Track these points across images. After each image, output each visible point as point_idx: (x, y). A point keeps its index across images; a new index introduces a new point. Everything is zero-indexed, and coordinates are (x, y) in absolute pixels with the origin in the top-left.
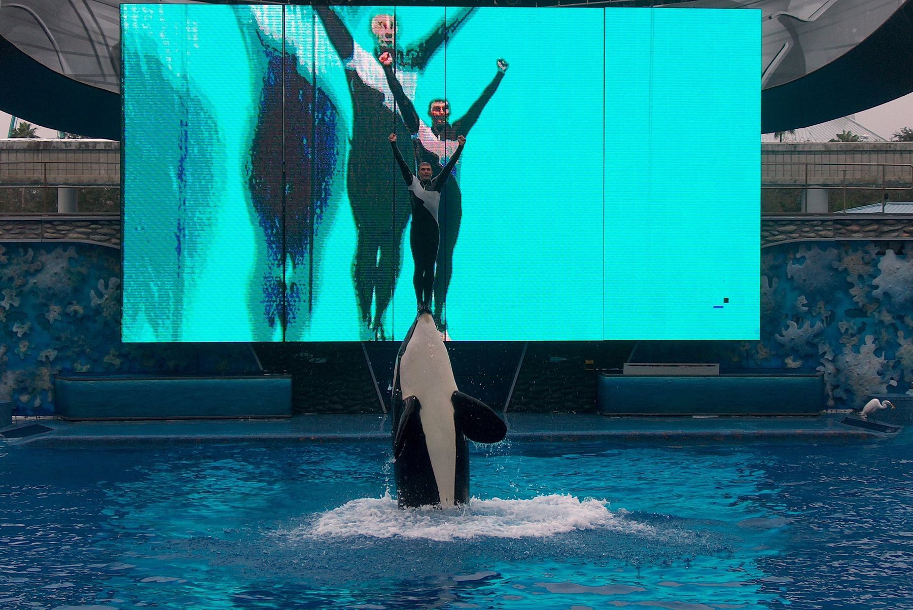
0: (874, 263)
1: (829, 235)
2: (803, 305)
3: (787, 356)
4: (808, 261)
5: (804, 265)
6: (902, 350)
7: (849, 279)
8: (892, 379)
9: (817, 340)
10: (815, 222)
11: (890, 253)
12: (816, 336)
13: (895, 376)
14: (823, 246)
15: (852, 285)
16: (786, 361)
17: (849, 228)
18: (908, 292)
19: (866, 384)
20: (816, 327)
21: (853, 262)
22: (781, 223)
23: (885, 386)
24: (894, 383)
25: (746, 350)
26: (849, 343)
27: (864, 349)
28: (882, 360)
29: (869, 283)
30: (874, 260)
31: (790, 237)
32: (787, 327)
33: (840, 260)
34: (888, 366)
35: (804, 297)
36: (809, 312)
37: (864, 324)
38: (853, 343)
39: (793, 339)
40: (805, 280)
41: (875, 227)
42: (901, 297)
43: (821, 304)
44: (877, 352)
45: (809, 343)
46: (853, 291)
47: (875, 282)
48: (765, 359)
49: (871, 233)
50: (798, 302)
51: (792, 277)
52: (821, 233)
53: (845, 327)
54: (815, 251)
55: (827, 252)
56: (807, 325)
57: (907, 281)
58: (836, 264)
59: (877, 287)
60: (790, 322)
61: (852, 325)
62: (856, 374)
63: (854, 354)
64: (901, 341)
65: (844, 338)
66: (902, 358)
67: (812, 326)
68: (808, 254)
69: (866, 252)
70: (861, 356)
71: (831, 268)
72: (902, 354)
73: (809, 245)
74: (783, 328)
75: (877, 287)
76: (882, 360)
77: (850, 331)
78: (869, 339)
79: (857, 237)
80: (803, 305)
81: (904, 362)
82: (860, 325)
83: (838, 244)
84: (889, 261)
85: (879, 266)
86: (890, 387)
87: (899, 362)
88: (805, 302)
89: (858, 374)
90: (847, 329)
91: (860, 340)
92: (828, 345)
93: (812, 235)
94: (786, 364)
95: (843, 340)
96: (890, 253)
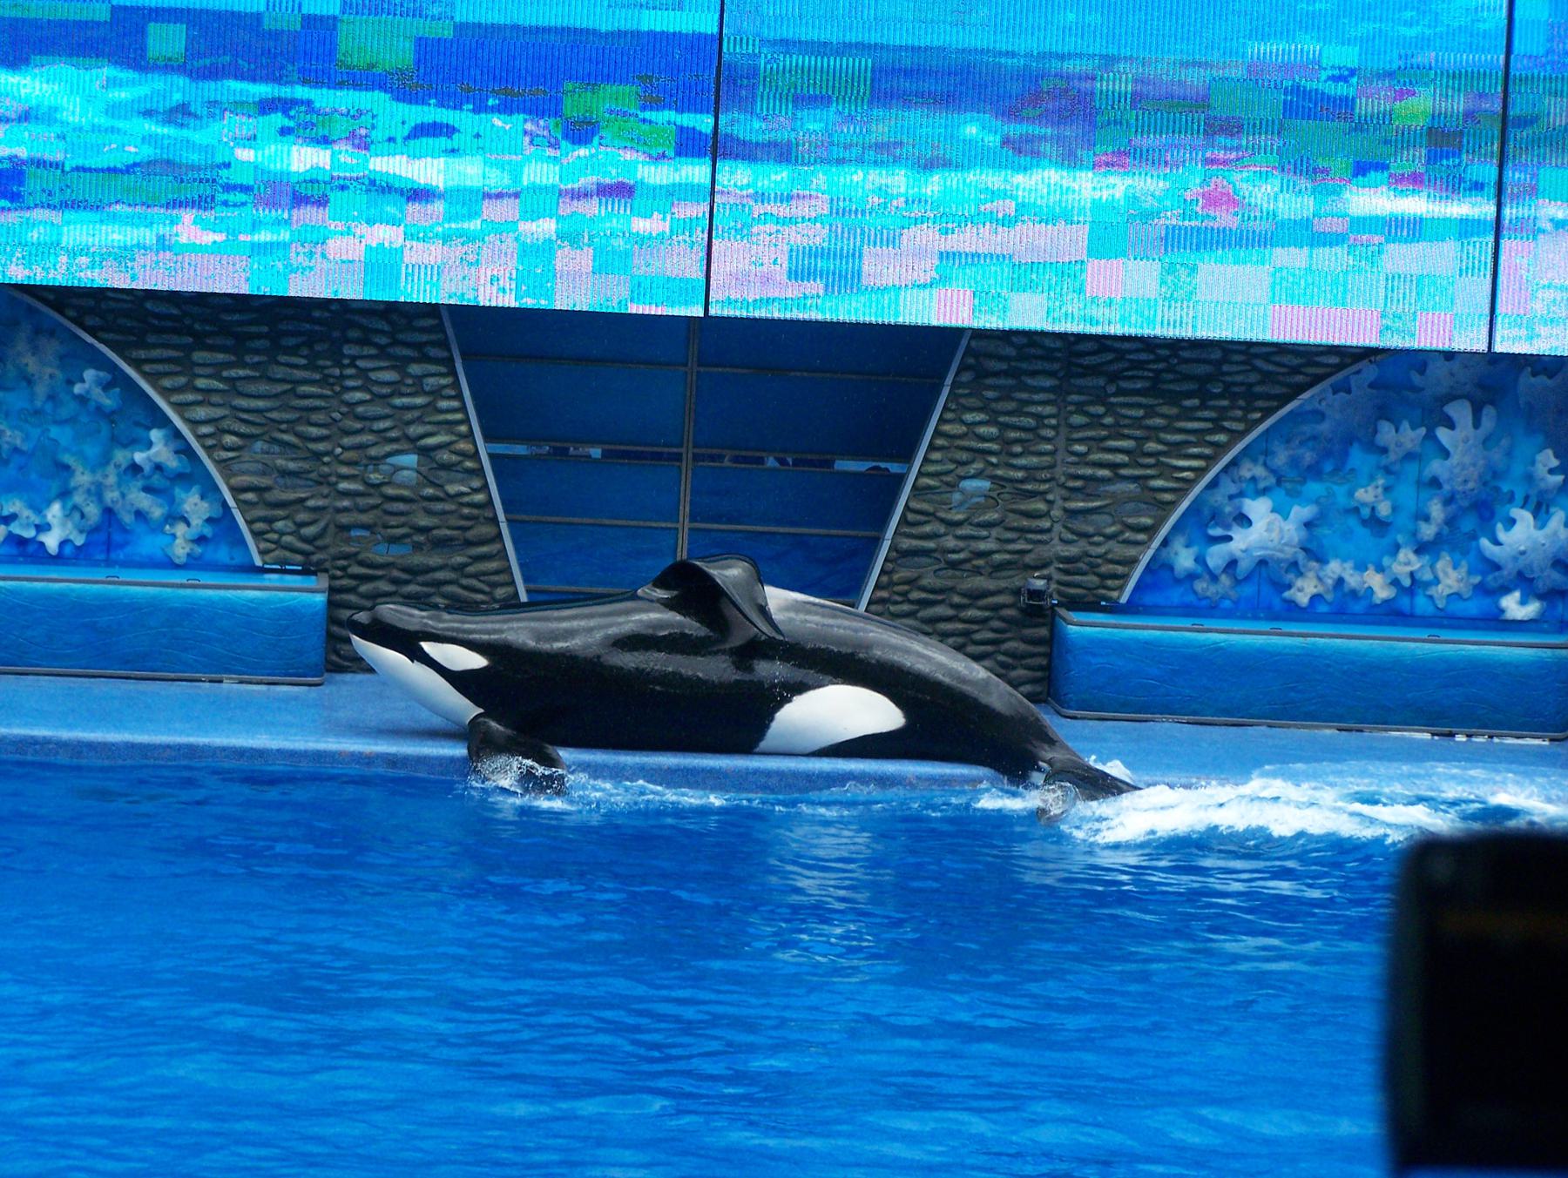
2: (1551, 471)
3: (1506, 590)
5: (1559, 379)
25: (1412, 574)
32: (1513, 522)
35: (1550, 452)
39: (1523, 553)
48: (1456, 596)
60: (1516, 512)
74: (1499, 526)
80: (1551, 471)
88: (1555, 463)
94: (1502, 611)
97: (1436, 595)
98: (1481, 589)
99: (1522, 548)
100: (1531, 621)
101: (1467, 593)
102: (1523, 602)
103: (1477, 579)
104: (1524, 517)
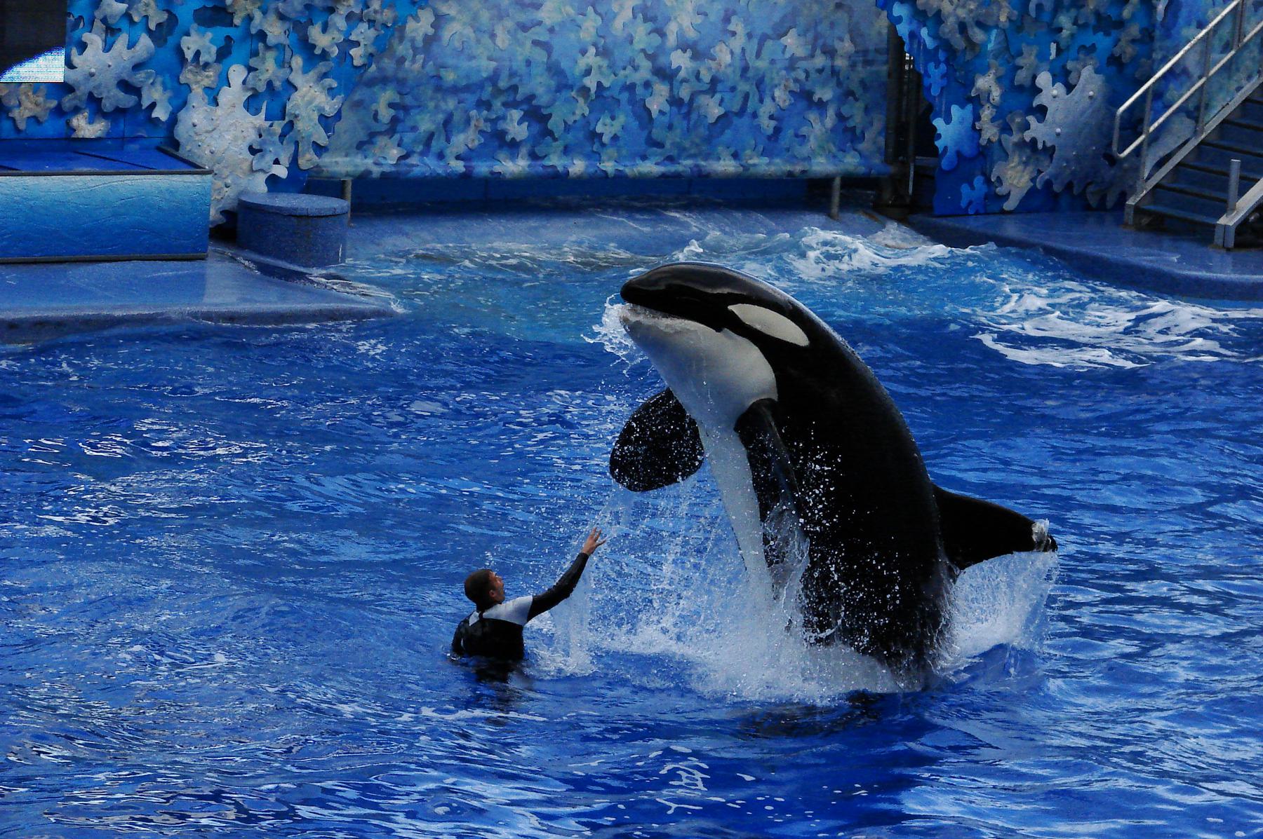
3: (76, 110)
6: (297, 98)
8: (277, 162)
9: (140, 76)
12: (137, 67)
13: (285, 159)
19: (226, 172)
20: (138, 48)
23: (261, 179)
24: (281, 171)
26: (197, 82)
27: (226, 96)
28: (260, 120)
34: (272, 134)
36: (127, 16)
37: (228, 38)
38: (206, 82)
39: (92, 75)
44: (251, 104)
48: (35, 119)
53: (194, 48)
56: (121, 41)
61: (207, 43)
62: (207, 152)
63: (208, 108)
64: (297, 79)
65: (190, 71)
66: (296, 116)
67: (131, 45)
70: (219, 111)
72: (297, 106)
76: (260, 120)
77: (203, 59)
78: (237, 74)
81: (299, 125)
82: (222, 44)
86: (273, 181)
87: (291, 124)
89: (212, 153)
90: (198, 54)
91: (219, 75)
92: (159, 88)
95: (187, 76)
98: (59, 112)
99: (93, 70)
100: (98, 139)
101: (44, 116)
102: (91, 122)
103: (53, 104)
104: (95, 40)
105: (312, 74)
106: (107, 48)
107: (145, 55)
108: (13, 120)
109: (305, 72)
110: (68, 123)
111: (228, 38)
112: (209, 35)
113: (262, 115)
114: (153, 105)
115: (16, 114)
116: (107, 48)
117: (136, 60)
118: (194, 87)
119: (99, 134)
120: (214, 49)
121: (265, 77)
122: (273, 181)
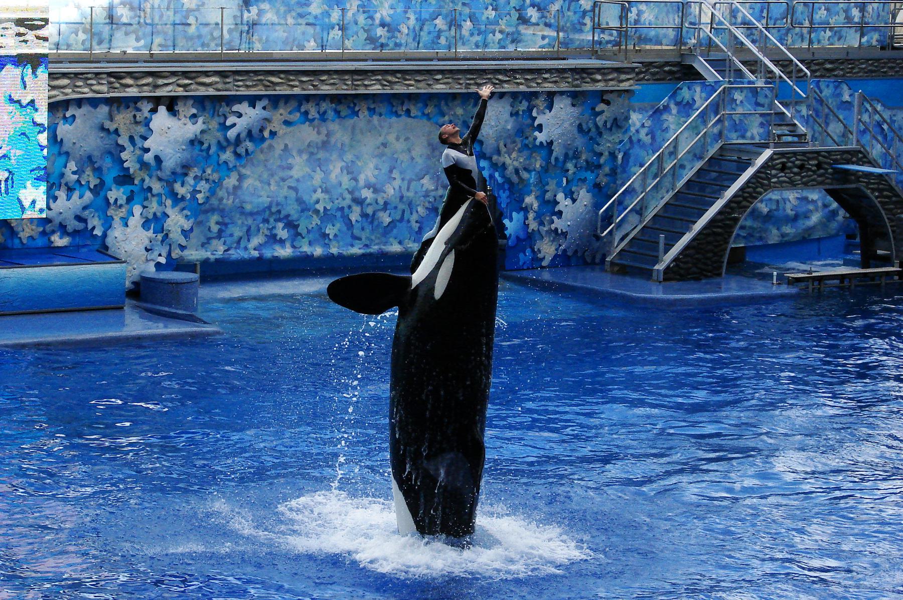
0: (147, 123)
1: (103, 89)
2: (74, 173)
3: (53, 232)
4: (78, 120)
7: (120, 142)
8: (160, 255)
9: (87, 212)
10: (89, 76)
11: (162, 109)
12: (85, 208)
13: (164, 254)
14: (94, 103)
15: (123, 149)
16: (53, 238)
17: (124, 81)
18: (179, 155)
19: (133, 262)
20: (85, 198)
21: (123, 119)
22: (54, 76)
23: (152, 264)
24: (163, 260)
26: (116, 215)
27: (132, 221)
28: (150, 233)
29: (140, 146)
30: (146, 118)
31: (63, 93)
33: (111, 119)
36: (78, 181)
37: (132, 191)
38: (121, 215)
39: (61, 213)
40: (74, 143)
41: (150, 80)
42: (171, 161)
43: (88, 171)
44: (146, 225)
45: (79, 218)
46: (124, 156)
47: (147, 144)
48: (31, 238)
49: (145, 88)
50: (68, 169)
51: (62, 140)
52: (94, 88)
53: (114, 197)
54: (85, 109)
55: (98, 109)
56: (76, 195)
57: (178, 142)
58: (108, 124)
59: (147, 150)
62: (123, 251)
63: (123, 228)
64: (169, 211)
67: (81, 197)
68: (78, 112)
69: (139, 110)
70: (128, 230)
71: (102, 128)
73: (79, 103)
75: (147, 150)
76: (150, 233)
77: (119, 203)
78: (137, 209)
79: (132, 92)
81: (171, 235)
83: (109, 101)
84: (161, 119)
85: (152, 125)
86: (158, 265)
87: (167, 235)
90: (116, 200)
91: (128, 211)
92: (97, 219)
93: (86, 90)
96: (162, 109)
97: (22, 237)
98: (44, 233)
100: (66, 247)
103: (41, 229)
105: (177, 209)
106: (69, 199)
107: (89, 202)
108: (20, 238)
109: (173, 207)
110: (49, 239)
111: (132, 191)
112: (122, 190)
113: (152, 231)
114: (94, 228)
115: (21, 235)
116: (69, 199)
117: (84, 205)
118: (115, 217)
119: (65, 244)
120: (125, 197)
121: (153, 210)
122: (158, 265)
